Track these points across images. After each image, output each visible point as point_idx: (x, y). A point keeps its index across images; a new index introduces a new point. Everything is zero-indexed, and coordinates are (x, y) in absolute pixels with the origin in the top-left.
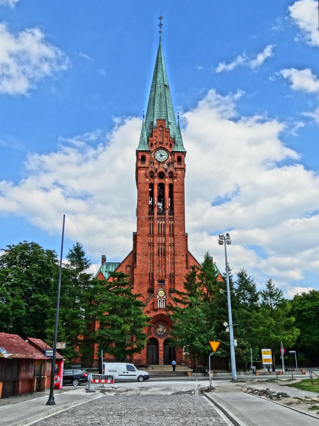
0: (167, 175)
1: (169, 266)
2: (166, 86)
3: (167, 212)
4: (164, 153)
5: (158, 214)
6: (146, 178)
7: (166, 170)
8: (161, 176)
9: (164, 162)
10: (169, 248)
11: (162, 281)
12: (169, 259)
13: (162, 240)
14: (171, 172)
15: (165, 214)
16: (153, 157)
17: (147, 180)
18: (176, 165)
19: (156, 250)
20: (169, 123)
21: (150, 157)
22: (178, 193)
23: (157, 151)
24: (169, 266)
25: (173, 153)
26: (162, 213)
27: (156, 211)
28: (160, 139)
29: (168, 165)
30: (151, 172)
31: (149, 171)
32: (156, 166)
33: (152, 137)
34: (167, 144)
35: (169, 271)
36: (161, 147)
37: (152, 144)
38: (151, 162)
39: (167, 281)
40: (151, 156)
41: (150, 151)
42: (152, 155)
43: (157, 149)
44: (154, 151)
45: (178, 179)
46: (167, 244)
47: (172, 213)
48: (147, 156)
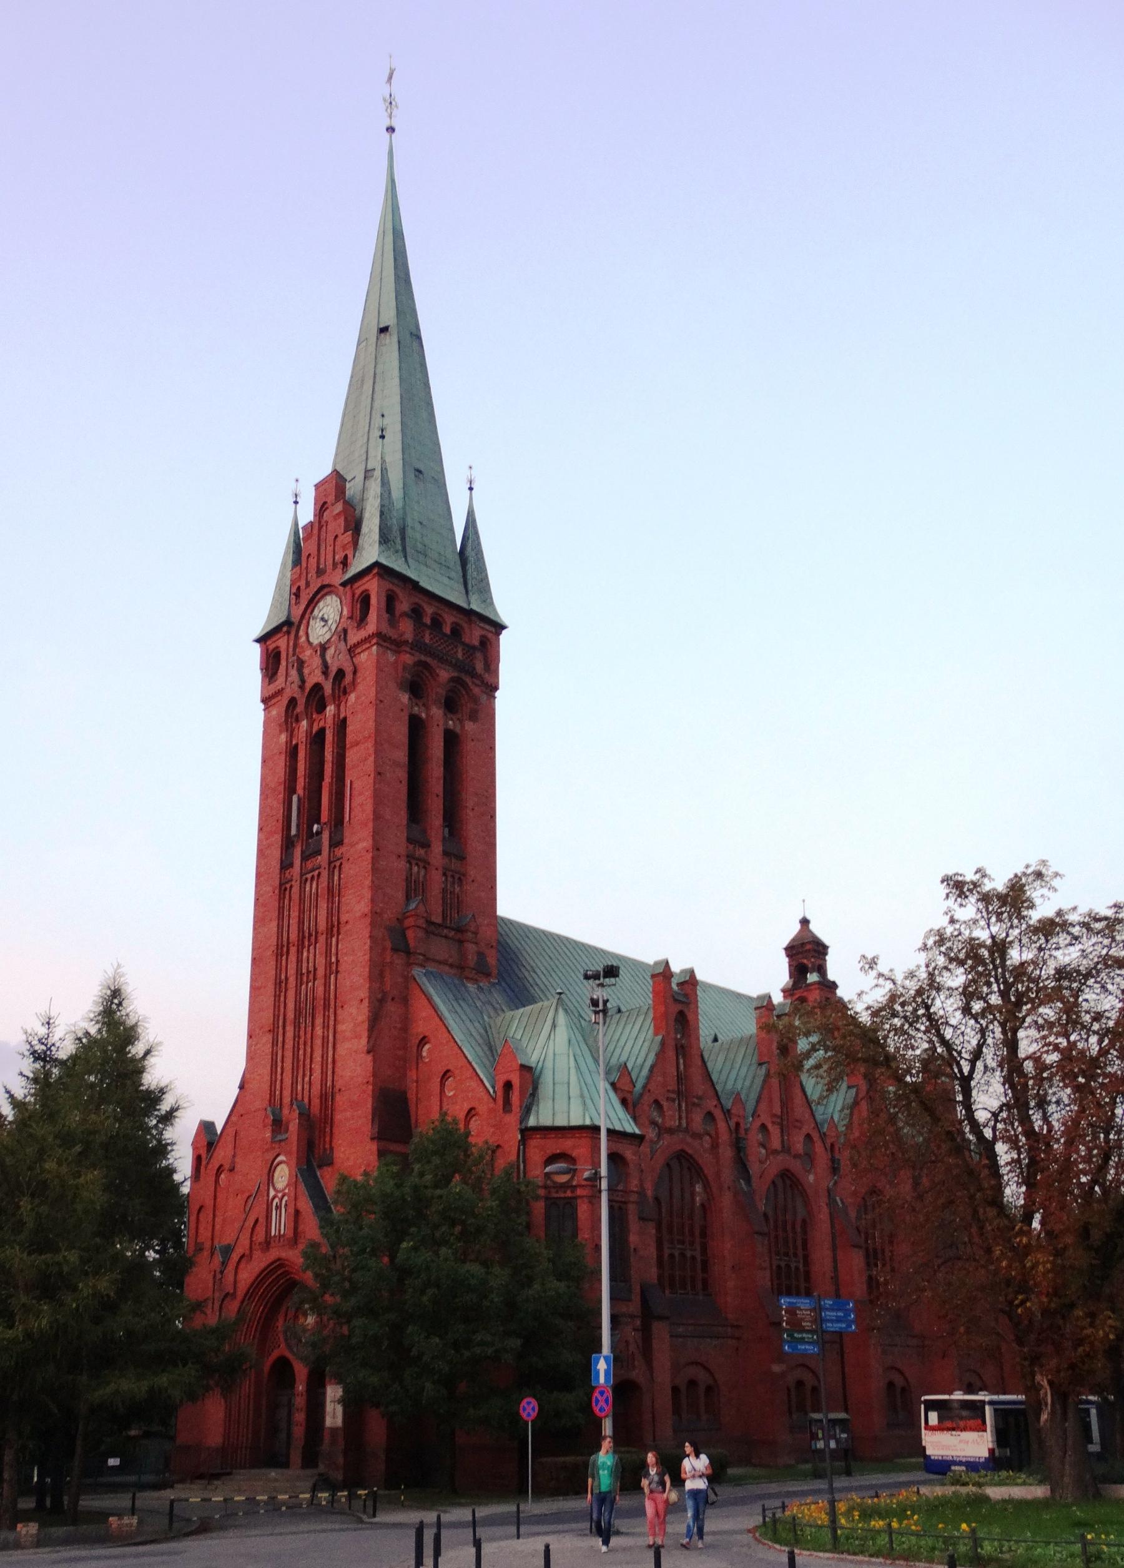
3: (326, 836)
4: (331, 609)
5: (305, 858)
6: (281, 732)
8: (316, 699)
9: (324, 648)
10: (326, 985)
14: (341, 673)
15: (319, 852)
16: (303, 639)
21: (296, 645)
22: (357, 744)
23: (313, 611)
30: (293, 702)
31: (285, 702)
36: (323, 587)
37: (299, 588)
40: (297, 637)
41: (288, 623)
42: (301, 633)
43: (313, 602)
44: (307, 616)
45: (360, 688)
46: (321, 972)
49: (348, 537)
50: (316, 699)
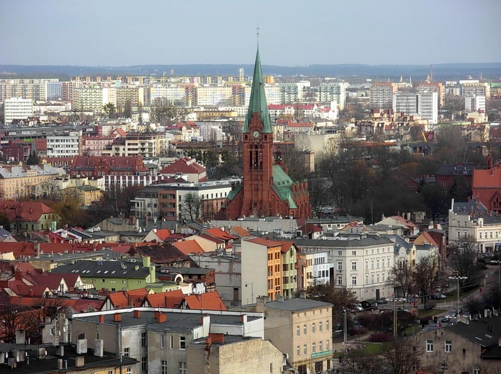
0: (259, 146)
1: (260, 196)
2: (260, 84)
3: (259, 167)
7: (258, 143)
11: (255, 204)
12: (260, 193)
13: (256, 182)
17: (249, 150)
18: (263, 141)
19: (253, 188)
20: (261, 112)
24: (260, 196)
25: (262, 134)
26: (256, 168)
27: (253, 167)
28: (255, 125)
29: (260, 140)
32: (253, 141)
33: (251, 123)
34: (259, 127)
35: (260, 198)
38: (250, 139)
39: (258, 205)
47: (261, 168)
48: (248, 135)
49: (262, 125)
50: (256, 147)
